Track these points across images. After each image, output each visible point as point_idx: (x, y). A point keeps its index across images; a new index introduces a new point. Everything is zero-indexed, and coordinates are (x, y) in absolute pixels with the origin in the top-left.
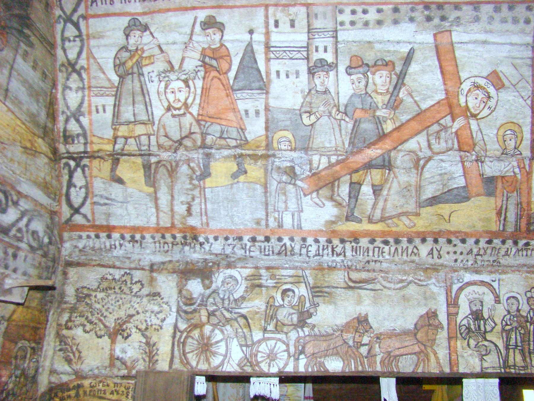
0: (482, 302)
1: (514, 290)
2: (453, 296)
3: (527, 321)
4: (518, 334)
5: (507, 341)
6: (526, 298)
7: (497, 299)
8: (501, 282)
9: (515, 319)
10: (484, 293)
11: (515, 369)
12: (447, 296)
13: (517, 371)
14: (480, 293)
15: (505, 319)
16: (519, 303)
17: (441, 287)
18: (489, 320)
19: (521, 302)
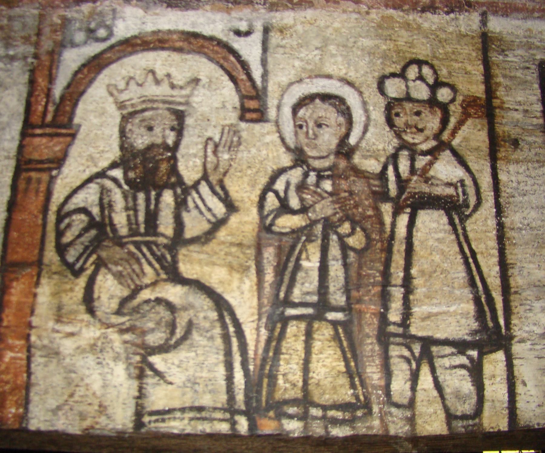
0: (180, 116)
1: (329, 69)
2: (58, 91)
3: (384, 196)
4: (335, 251)
5: (278, 284)
6: (382, 102)
7: (252, 104)
8: (275, 38)
9: (327, 185)
10: (196, 81)
11: (304, 417)
12: (30, 94)
13: (317, 430)
14: (180, 78)
15: (280, 186)
16: (350, 122)
17: (12, 59)
18: (204, 188)
19: (358, 115)
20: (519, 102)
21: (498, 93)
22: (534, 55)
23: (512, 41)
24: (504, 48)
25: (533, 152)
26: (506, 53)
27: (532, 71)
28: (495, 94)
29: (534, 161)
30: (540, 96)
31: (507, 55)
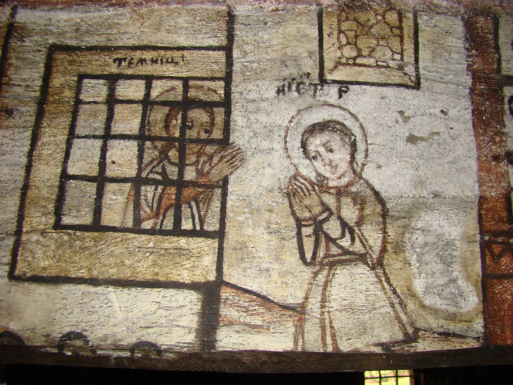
20: (24, 79)
21: (8, 72)
22: (47, 40)
23: (34, 29)
24: (24, 35)
25: (23, 119)
26: (25, 39)
27: (42, 53)
28: (6, 73)
29: (20, 127)
30: (43, 73)
31: (24, 41)
